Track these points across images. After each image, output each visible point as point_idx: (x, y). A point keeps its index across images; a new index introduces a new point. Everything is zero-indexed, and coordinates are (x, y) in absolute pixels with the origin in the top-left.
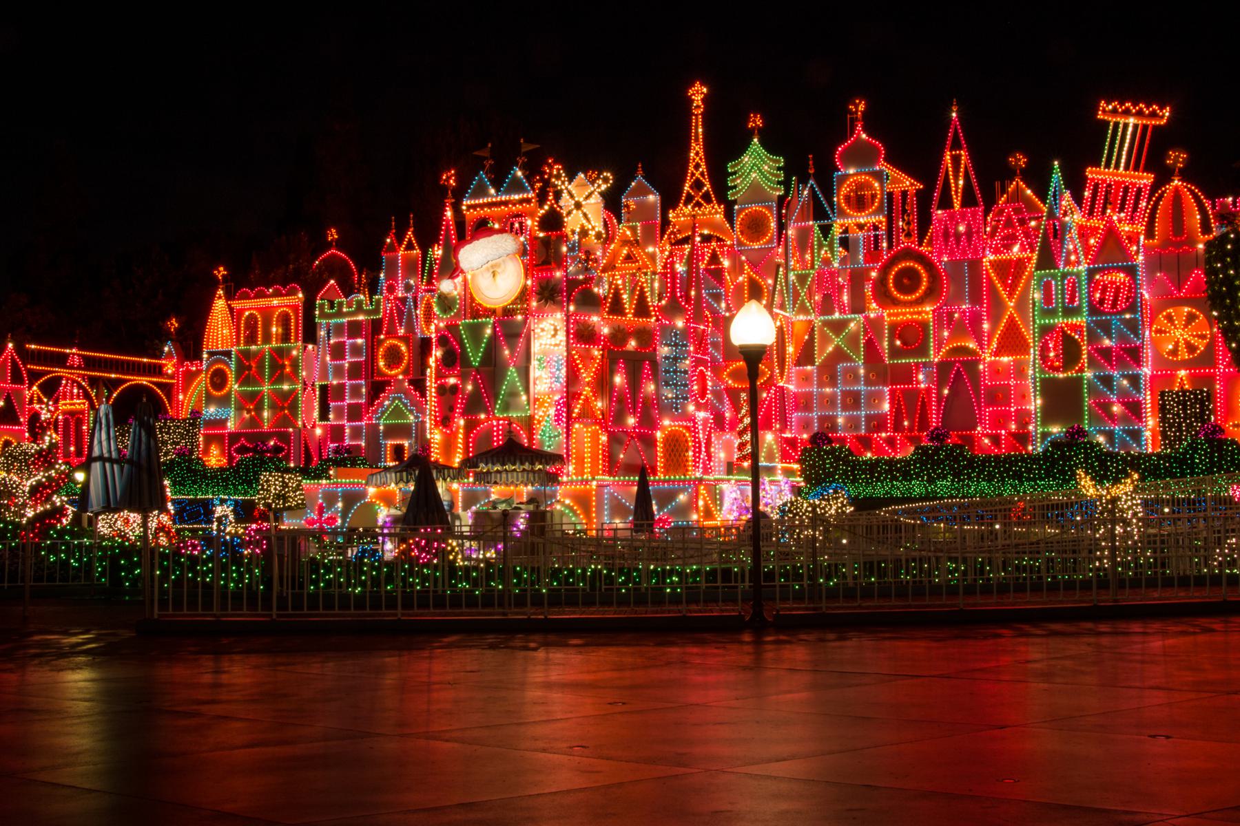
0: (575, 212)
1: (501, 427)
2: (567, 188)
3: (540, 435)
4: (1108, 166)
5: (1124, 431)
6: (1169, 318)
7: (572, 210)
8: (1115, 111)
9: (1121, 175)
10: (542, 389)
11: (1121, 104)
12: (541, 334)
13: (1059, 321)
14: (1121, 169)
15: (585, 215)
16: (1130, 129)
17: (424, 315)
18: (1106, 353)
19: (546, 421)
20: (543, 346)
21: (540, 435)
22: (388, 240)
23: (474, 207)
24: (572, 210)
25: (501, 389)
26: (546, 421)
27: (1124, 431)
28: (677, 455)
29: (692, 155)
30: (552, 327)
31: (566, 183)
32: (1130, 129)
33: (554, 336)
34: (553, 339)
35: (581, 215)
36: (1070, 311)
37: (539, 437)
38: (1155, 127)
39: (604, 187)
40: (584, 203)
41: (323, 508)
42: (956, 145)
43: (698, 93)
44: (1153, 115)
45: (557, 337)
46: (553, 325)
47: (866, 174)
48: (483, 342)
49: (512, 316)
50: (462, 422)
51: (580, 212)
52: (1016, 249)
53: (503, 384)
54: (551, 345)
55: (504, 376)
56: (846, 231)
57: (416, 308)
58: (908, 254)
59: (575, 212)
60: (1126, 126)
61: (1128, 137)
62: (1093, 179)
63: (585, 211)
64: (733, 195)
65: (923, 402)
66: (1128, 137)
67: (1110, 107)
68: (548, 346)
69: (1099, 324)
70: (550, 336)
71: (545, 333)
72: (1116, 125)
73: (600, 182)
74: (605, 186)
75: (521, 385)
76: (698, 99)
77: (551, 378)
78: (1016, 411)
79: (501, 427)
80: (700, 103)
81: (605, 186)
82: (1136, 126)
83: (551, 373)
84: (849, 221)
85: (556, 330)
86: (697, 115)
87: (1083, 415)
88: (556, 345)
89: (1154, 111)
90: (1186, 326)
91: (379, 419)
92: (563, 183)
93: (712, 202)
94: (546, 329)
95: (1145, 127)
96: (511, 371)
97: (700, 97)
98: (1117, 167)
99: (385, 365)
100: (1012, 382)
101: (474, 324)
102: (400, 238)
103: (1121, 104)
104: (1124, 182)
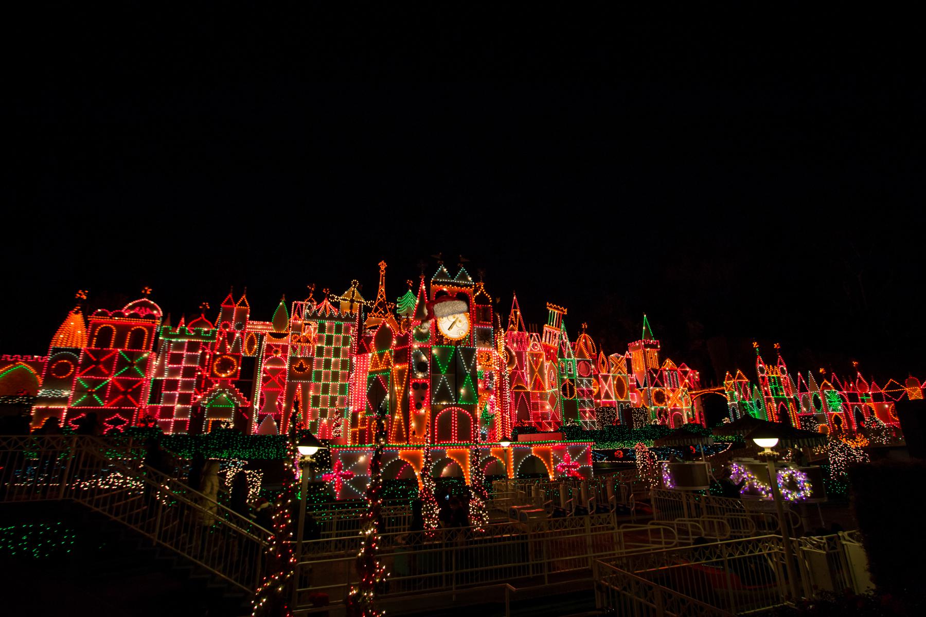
8: (551, 307)
16: (556, 313)
29: (379, 291)
32: (556, 313)
38: (563, 315)
41: (342, 466)
42: (515, 307)
43: (383, 265)
44: (562, 310)
60: (554, 313)
64: (399, 311)
76: (383, 268)
82: (557, 313)
88: (489, 366)
95: (560, 314)
97: (384, 267)
98: (553, 325)
100: (539, 401)
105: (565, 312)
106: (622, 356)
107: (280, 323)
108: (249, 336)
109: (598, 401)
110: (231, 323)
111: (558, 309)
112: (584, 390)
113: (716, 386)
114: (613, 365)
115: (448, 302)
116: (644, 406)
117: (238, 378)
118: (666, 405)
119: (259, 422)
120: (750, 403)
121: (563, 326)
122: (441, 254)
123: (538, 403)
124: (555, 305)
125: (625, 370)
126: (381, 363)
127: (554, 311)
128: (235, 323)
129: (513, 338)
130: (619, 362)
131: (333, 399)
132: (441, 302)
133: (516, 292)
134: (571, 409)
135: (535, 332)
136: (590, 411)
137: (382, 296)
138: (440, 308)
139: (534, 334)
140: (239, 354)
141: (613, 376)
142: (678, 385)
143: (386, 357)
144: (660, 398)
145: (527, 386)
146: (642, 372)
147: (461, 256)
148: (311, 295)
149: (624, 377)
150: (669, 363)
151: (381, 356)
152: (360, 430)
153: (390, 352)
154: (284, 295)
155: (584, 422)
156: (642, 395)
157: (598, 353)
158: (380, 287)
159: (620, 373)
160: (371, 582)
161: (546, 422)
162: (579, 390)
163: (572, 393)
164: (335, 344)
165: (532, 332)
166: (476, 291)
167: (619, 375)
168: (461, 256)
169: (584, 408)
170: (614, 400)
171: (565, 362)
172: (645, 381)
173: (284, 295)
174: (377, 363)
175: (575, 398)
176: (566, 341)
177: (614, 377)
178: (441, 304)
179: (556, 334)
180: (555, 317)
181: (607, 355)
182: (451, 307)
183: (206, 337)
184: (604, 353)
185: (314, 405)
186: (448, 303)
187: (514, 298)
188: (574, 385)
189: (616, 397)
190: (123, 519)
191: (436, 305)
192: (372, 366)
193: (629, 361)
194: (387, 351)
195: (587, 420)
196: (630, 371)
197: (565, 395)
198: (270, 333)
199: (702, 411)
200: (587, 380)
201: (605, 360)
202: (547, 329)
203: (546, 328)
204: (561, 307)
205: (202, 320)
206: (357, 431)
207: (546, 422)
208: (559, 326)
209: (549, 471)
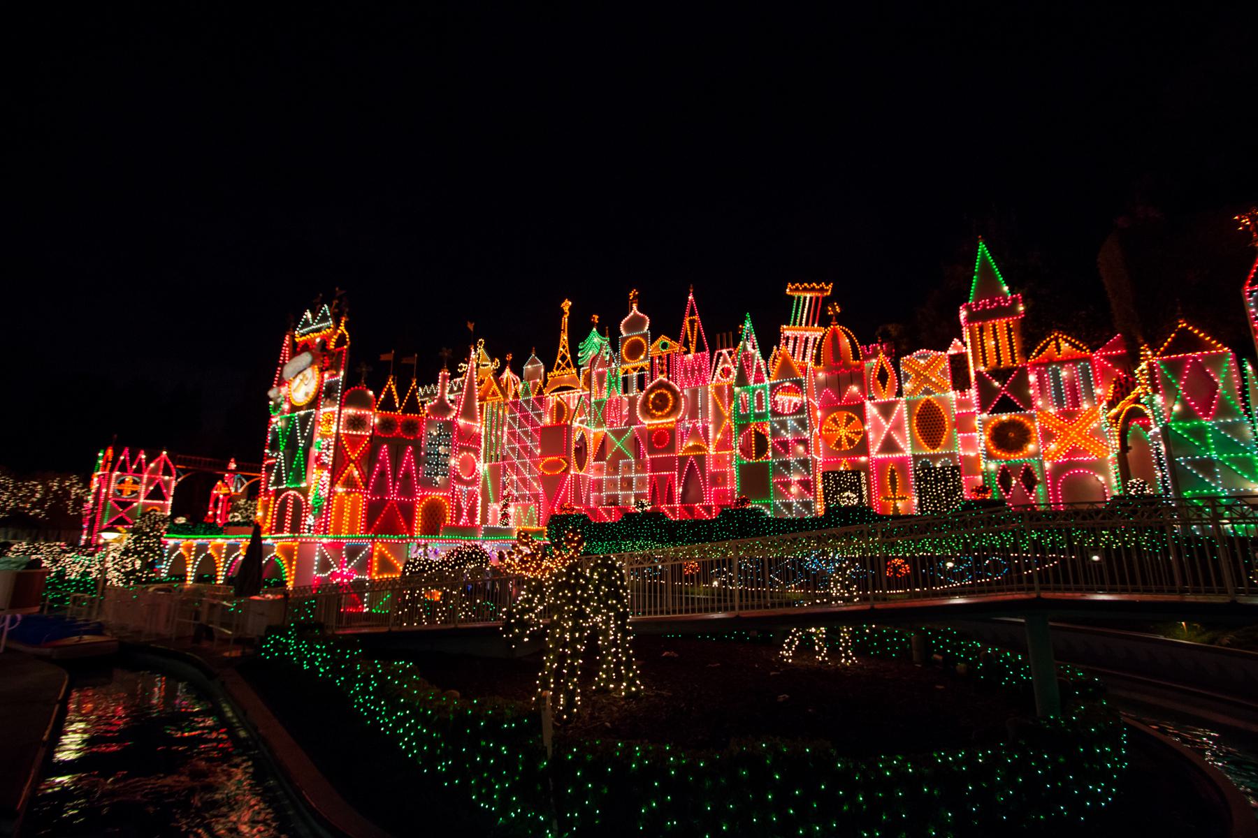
4: (794, 324)
6: (834, 420)
8: (797, 289)
11: (801, 284)
14: (803, 325)
23: (303, 335)
28: (436, 519)
43: (567, 305)
44: (822, 290)
47: (638, 335)
56: (626, 372)
58: (661, 385)
65: (670, 485)
72: (799, 298)
76: (566, 309)
82: (811, 298)
84: (627, 366)
87: (769, 490)
90: (846, 426)
95: (817, 298)
98: (801, 324)
103: (801, 284)
105: (827, 290)
109: (863, 459)
112: (788, 440)
120: (1225, 427)
123: (726, 472)
124: (806, 284)
127: (804, 295)
129: (685, 366)
133: (694, 288)
134: (755, 479)
136: (800, 482)
137: (564, 347)
139: (724, 351)
141: (908, 402)
145: (708, 445)
158: (562, 335)
159: (928, 392)
160: (565, 717)
161: (701, 507)
162: (777, 442)
165: (722, 348)
169: (785, 476)
170: (908, 452)
171: (748, 392)
176: (753, 351)
177: (911, 405)
179: (807, 338)
187: (690, 298)
189: (915, 445)
190: (644, 613)
195: (792, 500)
200: (796, 420)
201: (889, 369)
202: (788, 333)
203: (787, 331)
207: (701, 507)
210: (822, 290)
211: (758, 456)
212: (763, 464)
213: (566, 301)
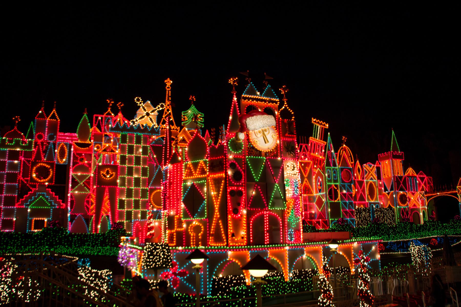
0: (146, 117)
1: (267, 215)
2: (142, 106)
3: (289, 219)
5: (350, 220)
7: (145, 116)
9: (317, 141)
10: (289, 196)
12: (288, 168)
13: (333, 184)
15: (151, 119)
17: (59, 152)
18: (345, 194)
19: (291, 212)
20: (288, 174)
21: (289, 219)
22: (40, 112)
24: (145, 116)
25: (271, 195)
26: (291, 212)
27: (350, 220)
30: (292, 165)
31: (142, 104)
32: (319, 128)
33: (293, 170)
34: (293, 171)
35: (149, 119)
36: (336, 181)
37: (288, 220)
38: (325, 129)
39: (161, 109)
40: (150, 114)
43: (169, 82)
44: (324, 125)
45: (295, 170)
46: (293, 164)
48: (253, 171)
49: (276, 158)
50: (245, 212)
51: (148, 117)
52: (306, 159)
53: (272, 192)
54: (292, 174)
55: (273, 188)
57: (55, 149)
59: (146, 117)
60: (318, 127)
61: (319, 130)
62: (311, 141)
63: (151, 117)
66: (319, 130)
67: (314, 120)
68: (291, 175)
69: (342, 185)
70: (291, 170)
71: (289, 168)
72: (316, 126)
73: (159, 106)
74: (162, 109)
75: (282, 193)
77: (293, 191)
78: (309, 213)
79: (267, 215)
80: (169, 86)
81: (162, 109)
83: (293, 188)
85: (294, 167)
86: (169, 91)
88: (294, 174)
89: (324, 124)
91: (28, 205)
92: (141, 103)
93: (174, 125)
94: (289, 166)
95: (322, 128)
96: (276, 186)
98: (317, 138)
99: (36, 176)
101: (256, 159)
102: (47, 112)
104: (318, 143)
106: (373, 165)
107: (84, 134)
108: (60, 146)
110: (44, 133)
111: (321, 124)
113: (449, 190)
114: (366, 172)
115: (259, 116)
116: (390, 207)
117: (53, 184)
118: (407, 205)
119: (71, 221)
121: (329, 138)
122: (248, 71)
124: (318, 120)
125: (376, 177)
126: (196, 173)
128: (47, 135)
130: (371, 170)
131: (137, 202)
132: (253, 116)
135: (305, 143)
138: (252, 122)
140: (53, 162)
142: (417, 190)
143: (200, 166)
144: (404, 199)
146: (389, 179)
147: (265, 74)
148: (109, 109)
149: (375, 182)
150: (410, 171)
151: (195, 165)
152: (177, 232)
153: (205, 162)
154: (86, 109)
155: (351, 220)
156: (389, 197)
157: (355, 162)
159: (371, 179)
163: (336, 197)
164: (136, 154)
166: (280, 107)
167: (371, 181)
168: (265, 74)
170: (367, 201)
172: (392, 184)
173: (86, 109)
174: (191, 172)
175: (339, 200)
178: (253, 117)
180: (318, 132)
181: (361, 164)
182: (261, 121)
183: (9, 145)
184: (359, 162)
185: (120, 208)
186: (259, 117)
188: (338, 189)
191: (248, 119)
192: (186, 174)
193: (378, 169)
194: (201, 161)
196: (379, 178)
197: (331, 198)
198: (76, 143)
199: (434, 209)
204: (323, 122)
205: (15, 131)
206: (174, 233)
208: (325, 139)
209: (350, 265)
210: (324, 125)
211: (335, 199)
212: (336, 203)
213: (169, 79)
